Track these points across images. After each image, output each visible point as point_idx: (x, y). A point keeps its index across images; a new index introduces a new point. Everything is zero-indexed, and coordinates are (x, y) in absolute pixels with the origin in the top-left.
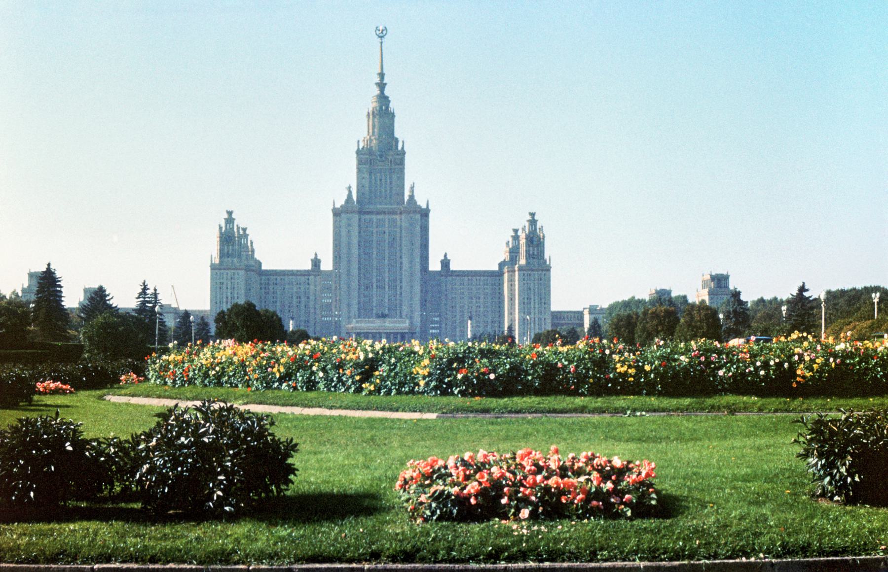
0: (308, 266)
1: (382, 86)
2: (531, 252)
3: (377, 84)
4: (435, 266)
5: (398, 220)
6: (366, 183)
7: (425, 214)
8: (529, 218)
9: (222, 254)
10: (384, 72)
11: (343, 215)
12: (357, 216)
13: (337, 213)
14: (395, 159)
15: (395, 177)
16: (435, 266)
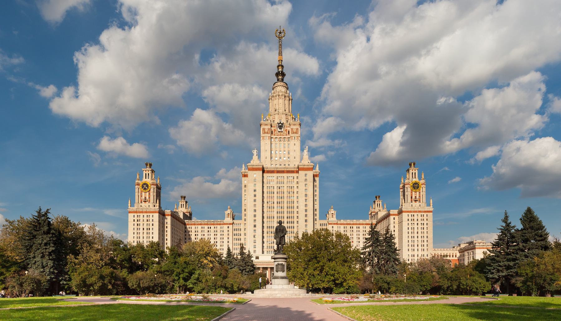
2: (414, 197)
5: (295, 178)
12: (261, 172)
14: (292, 129)
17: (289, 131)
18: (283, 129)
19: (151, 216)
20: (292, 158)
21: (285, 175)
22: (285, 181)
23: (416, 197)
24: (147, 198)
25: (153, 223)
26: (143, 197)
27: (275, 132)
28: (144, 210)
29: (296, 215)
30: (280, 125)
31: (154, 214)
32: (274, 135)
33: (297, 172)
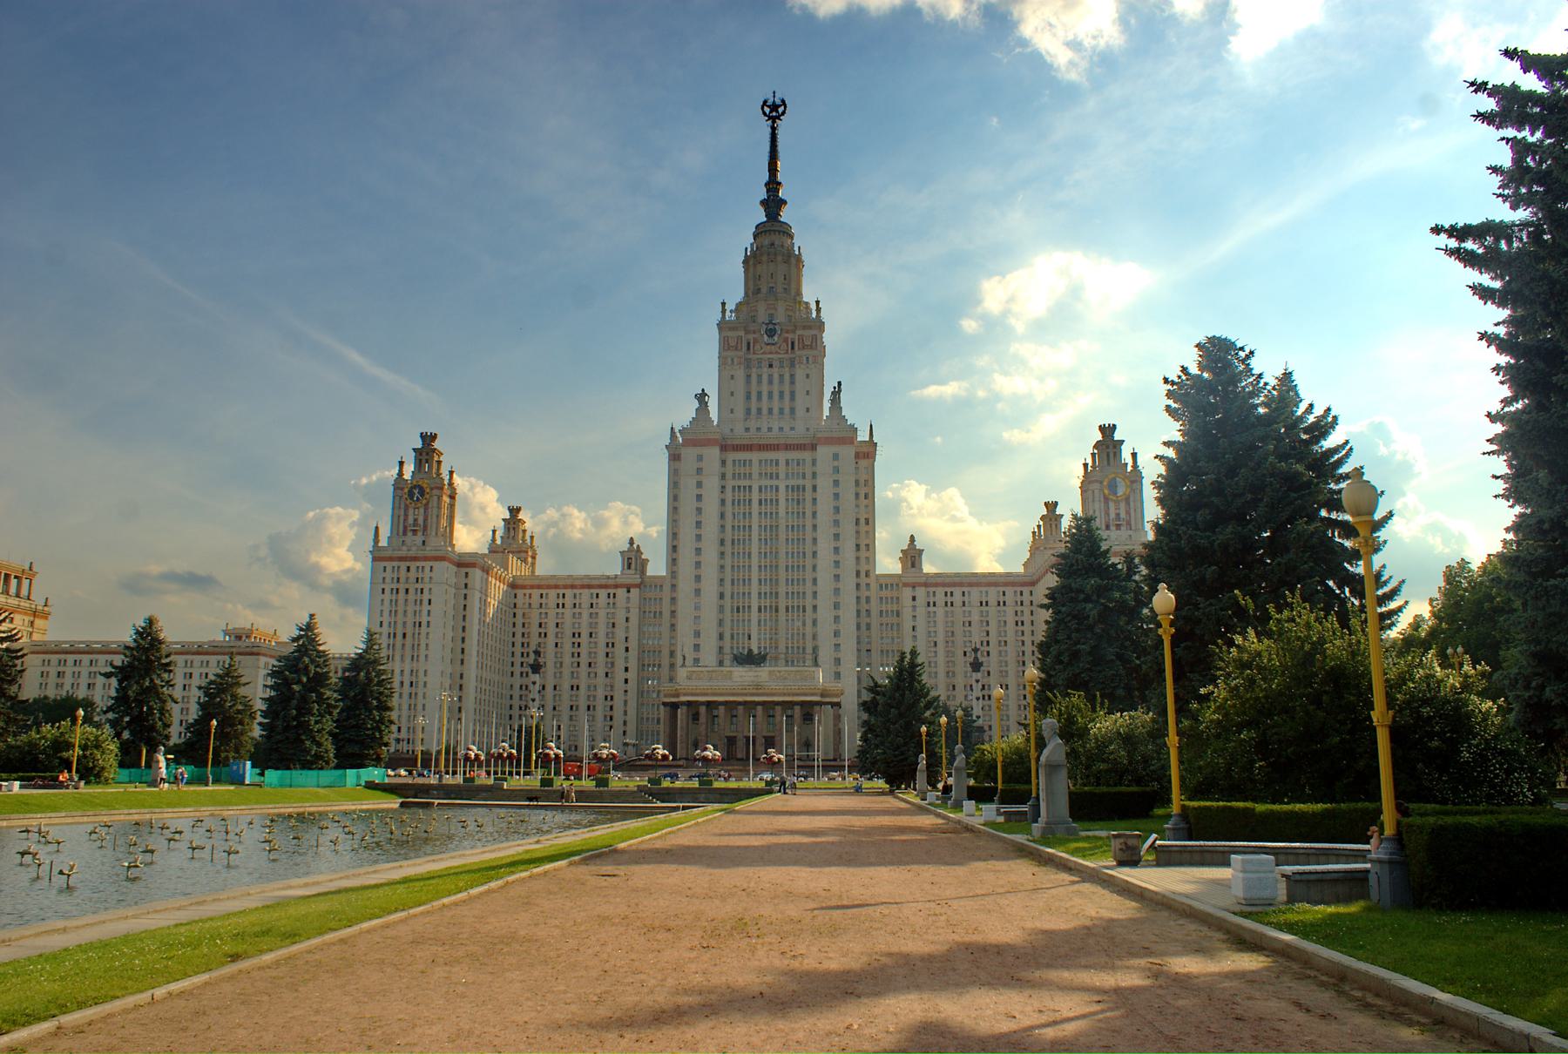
0: (615, 568)
1: (773, 204)
2: (1112, 515)
3: (763, 203)
4: (888, 563)
6: (739, 386)
7: (868, 452)
8: (1099, 437)
9: (402, 527)
10: (779, 178)
11: (689, 454)
12: (714, 452)
13: (675, 457)
14: (801, 338)
15: (800, 373)
16: (888, 563)
17: (793, 343)
18: (776, 338)
19: (427, 569)
20: (800, 412)
21: (781, 456)
22: (782, 469)
23: (1118, 515)
24: (421, 521)
25: (430, 586)
26: (411, 520)
27: (758, 347)
28: (412, 553)
29: (809, 562)
30: (771, 326)
31: (436, 564)
32: (754, 353)
33: (813, 447)
